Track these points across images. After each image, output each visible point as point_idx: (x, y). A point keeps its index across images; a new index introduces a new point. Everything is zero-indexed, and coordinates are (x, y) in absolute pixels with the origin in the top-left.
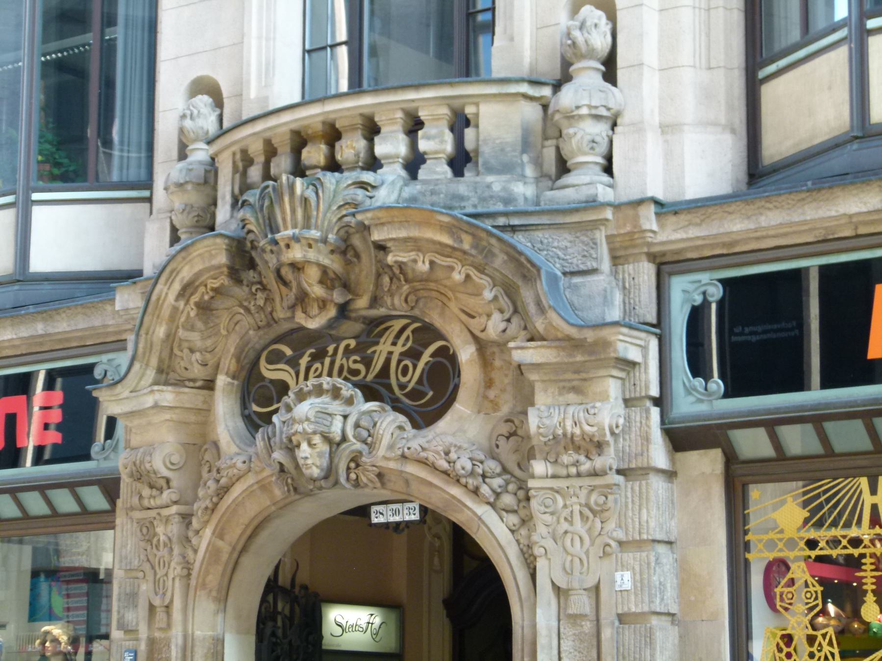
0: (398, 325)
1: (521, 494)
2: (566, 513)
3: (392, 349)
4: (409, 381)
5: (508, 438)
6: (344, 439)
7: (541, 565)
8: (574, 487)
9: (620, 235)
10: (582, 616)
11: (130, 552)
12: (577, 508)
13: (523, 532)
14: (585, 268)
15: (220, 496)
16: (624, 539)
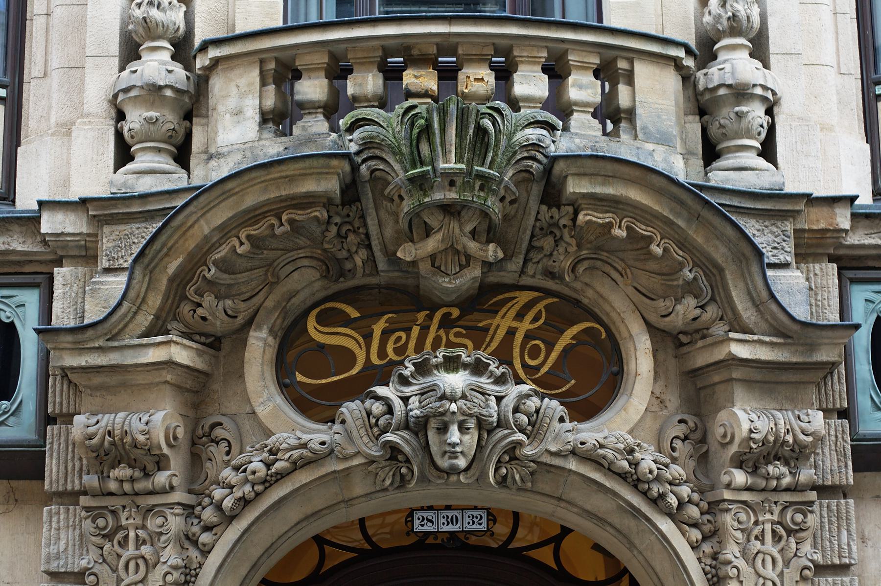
0: (524, 297)
1: (704, 505)
2: (757, 530)
5: (683, 441)
6: (501, 423)
8: (769, 500)
9: (811, 231)
11: (66, 549)
12: (768, 527)
13: (707, 548)
14: (777, 261)
15: (267, 485)
16: (822, 563)
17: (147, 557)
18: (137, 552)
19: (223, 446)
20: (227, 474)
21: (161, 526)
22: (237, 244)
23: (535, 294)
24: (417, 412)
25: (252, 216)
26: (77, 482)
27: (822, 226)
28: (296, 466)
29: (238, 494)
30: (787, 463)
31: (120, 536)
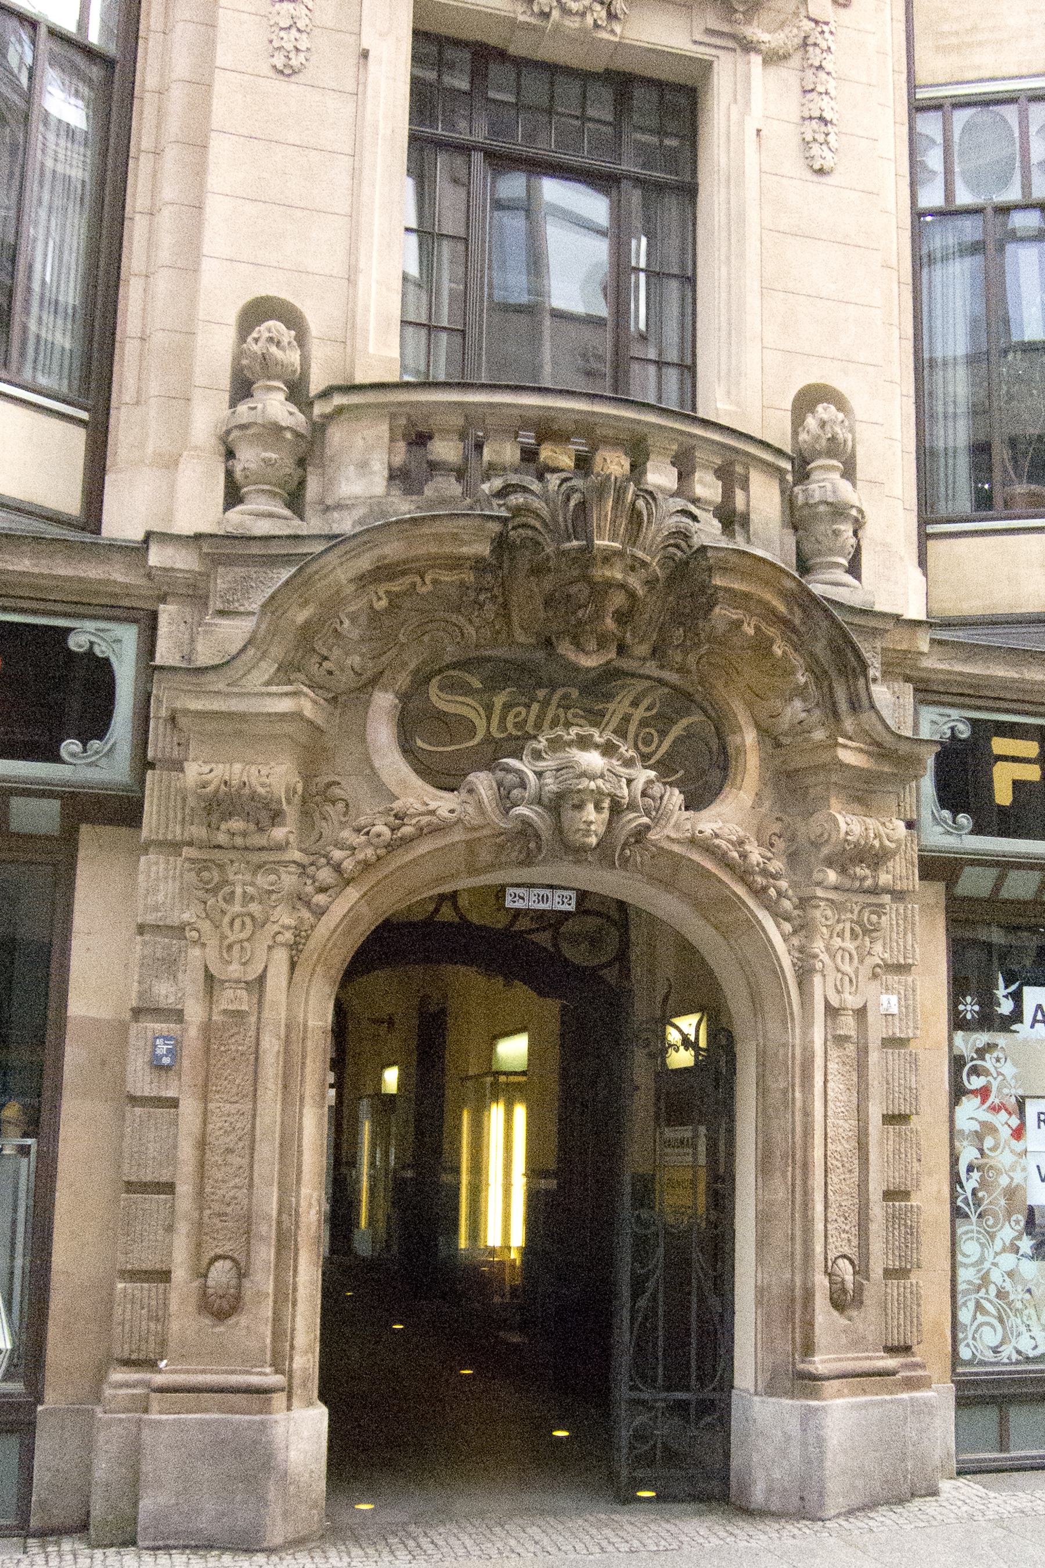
1: (796, 900)
3: (631, 710)
4: (655, 752)
7: (817, 979)
9: (895, 650)
10: (846, 1038)
12: (848, 925)
13: (795, 941)
17: (256, 915)
18: (244, 910)
19: (340, 805)
20: (346, 834)
21: (272, 884)
22: (375, 599)
23: (647, 683)
24: (554, 788)
25: (383, 572)
26: (178, 831)
27: (904, 646)
28: (421, 833)
29: (361, 856)
30: (868, 867)
31: (227, 889)
